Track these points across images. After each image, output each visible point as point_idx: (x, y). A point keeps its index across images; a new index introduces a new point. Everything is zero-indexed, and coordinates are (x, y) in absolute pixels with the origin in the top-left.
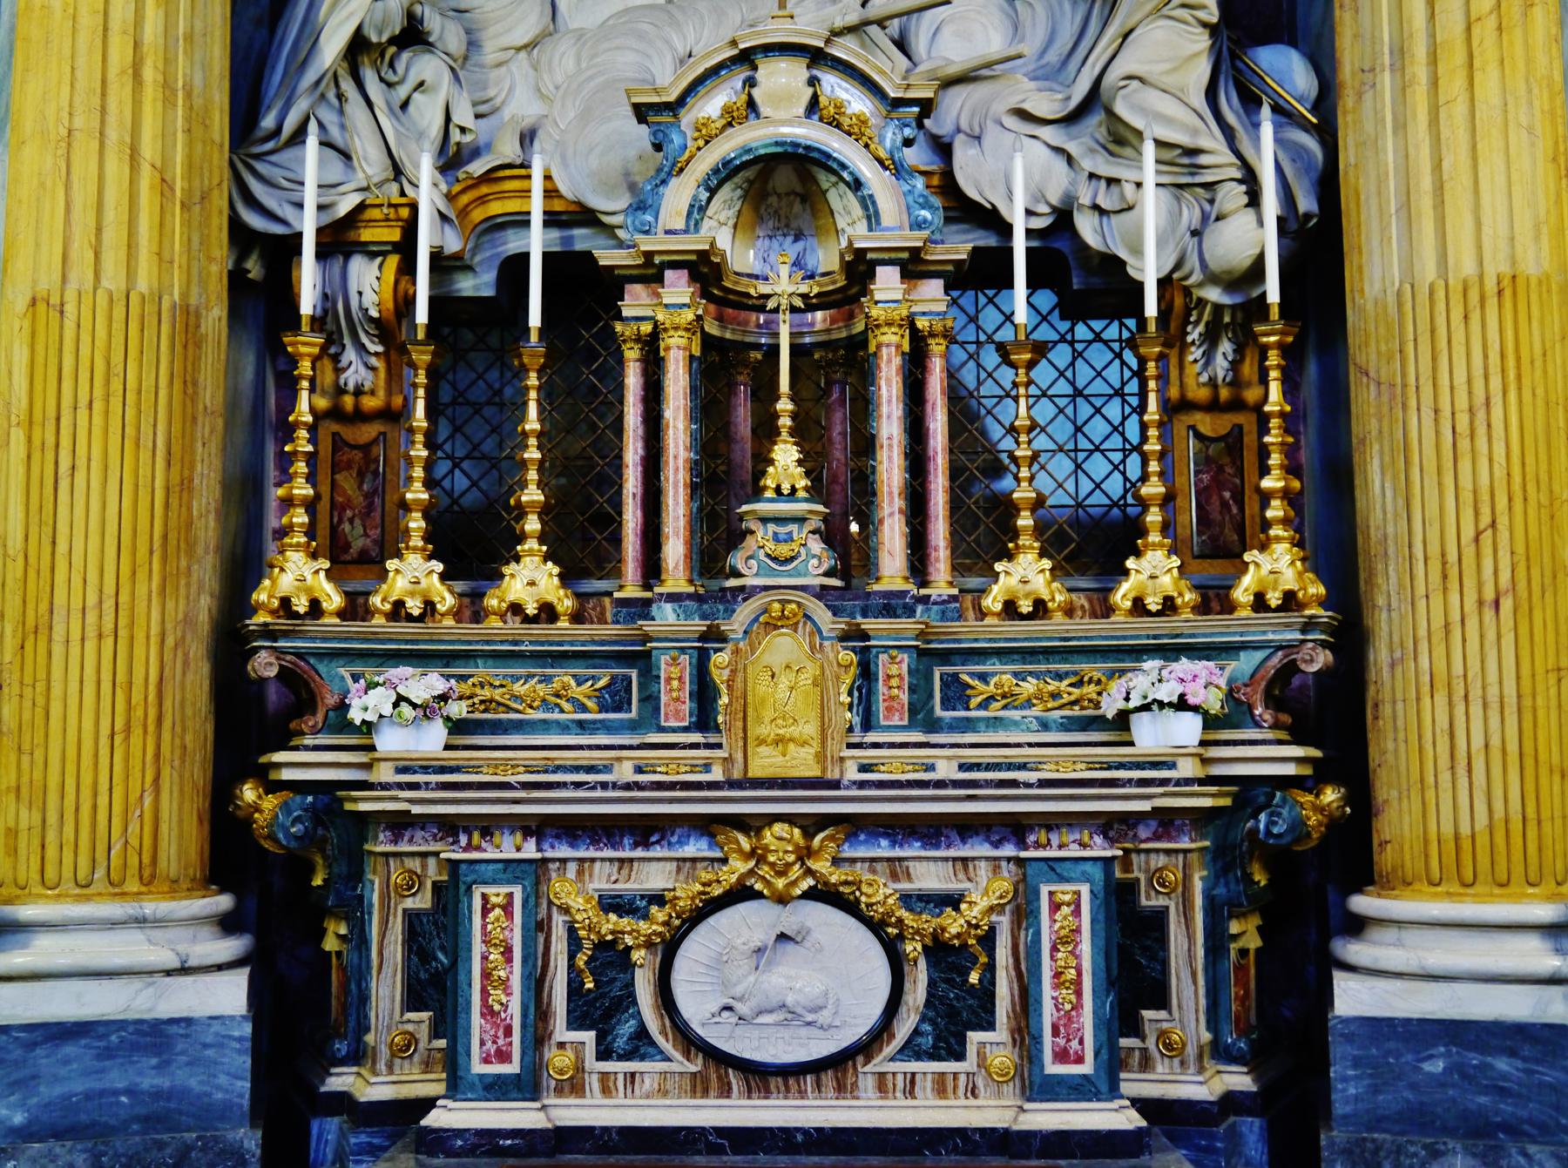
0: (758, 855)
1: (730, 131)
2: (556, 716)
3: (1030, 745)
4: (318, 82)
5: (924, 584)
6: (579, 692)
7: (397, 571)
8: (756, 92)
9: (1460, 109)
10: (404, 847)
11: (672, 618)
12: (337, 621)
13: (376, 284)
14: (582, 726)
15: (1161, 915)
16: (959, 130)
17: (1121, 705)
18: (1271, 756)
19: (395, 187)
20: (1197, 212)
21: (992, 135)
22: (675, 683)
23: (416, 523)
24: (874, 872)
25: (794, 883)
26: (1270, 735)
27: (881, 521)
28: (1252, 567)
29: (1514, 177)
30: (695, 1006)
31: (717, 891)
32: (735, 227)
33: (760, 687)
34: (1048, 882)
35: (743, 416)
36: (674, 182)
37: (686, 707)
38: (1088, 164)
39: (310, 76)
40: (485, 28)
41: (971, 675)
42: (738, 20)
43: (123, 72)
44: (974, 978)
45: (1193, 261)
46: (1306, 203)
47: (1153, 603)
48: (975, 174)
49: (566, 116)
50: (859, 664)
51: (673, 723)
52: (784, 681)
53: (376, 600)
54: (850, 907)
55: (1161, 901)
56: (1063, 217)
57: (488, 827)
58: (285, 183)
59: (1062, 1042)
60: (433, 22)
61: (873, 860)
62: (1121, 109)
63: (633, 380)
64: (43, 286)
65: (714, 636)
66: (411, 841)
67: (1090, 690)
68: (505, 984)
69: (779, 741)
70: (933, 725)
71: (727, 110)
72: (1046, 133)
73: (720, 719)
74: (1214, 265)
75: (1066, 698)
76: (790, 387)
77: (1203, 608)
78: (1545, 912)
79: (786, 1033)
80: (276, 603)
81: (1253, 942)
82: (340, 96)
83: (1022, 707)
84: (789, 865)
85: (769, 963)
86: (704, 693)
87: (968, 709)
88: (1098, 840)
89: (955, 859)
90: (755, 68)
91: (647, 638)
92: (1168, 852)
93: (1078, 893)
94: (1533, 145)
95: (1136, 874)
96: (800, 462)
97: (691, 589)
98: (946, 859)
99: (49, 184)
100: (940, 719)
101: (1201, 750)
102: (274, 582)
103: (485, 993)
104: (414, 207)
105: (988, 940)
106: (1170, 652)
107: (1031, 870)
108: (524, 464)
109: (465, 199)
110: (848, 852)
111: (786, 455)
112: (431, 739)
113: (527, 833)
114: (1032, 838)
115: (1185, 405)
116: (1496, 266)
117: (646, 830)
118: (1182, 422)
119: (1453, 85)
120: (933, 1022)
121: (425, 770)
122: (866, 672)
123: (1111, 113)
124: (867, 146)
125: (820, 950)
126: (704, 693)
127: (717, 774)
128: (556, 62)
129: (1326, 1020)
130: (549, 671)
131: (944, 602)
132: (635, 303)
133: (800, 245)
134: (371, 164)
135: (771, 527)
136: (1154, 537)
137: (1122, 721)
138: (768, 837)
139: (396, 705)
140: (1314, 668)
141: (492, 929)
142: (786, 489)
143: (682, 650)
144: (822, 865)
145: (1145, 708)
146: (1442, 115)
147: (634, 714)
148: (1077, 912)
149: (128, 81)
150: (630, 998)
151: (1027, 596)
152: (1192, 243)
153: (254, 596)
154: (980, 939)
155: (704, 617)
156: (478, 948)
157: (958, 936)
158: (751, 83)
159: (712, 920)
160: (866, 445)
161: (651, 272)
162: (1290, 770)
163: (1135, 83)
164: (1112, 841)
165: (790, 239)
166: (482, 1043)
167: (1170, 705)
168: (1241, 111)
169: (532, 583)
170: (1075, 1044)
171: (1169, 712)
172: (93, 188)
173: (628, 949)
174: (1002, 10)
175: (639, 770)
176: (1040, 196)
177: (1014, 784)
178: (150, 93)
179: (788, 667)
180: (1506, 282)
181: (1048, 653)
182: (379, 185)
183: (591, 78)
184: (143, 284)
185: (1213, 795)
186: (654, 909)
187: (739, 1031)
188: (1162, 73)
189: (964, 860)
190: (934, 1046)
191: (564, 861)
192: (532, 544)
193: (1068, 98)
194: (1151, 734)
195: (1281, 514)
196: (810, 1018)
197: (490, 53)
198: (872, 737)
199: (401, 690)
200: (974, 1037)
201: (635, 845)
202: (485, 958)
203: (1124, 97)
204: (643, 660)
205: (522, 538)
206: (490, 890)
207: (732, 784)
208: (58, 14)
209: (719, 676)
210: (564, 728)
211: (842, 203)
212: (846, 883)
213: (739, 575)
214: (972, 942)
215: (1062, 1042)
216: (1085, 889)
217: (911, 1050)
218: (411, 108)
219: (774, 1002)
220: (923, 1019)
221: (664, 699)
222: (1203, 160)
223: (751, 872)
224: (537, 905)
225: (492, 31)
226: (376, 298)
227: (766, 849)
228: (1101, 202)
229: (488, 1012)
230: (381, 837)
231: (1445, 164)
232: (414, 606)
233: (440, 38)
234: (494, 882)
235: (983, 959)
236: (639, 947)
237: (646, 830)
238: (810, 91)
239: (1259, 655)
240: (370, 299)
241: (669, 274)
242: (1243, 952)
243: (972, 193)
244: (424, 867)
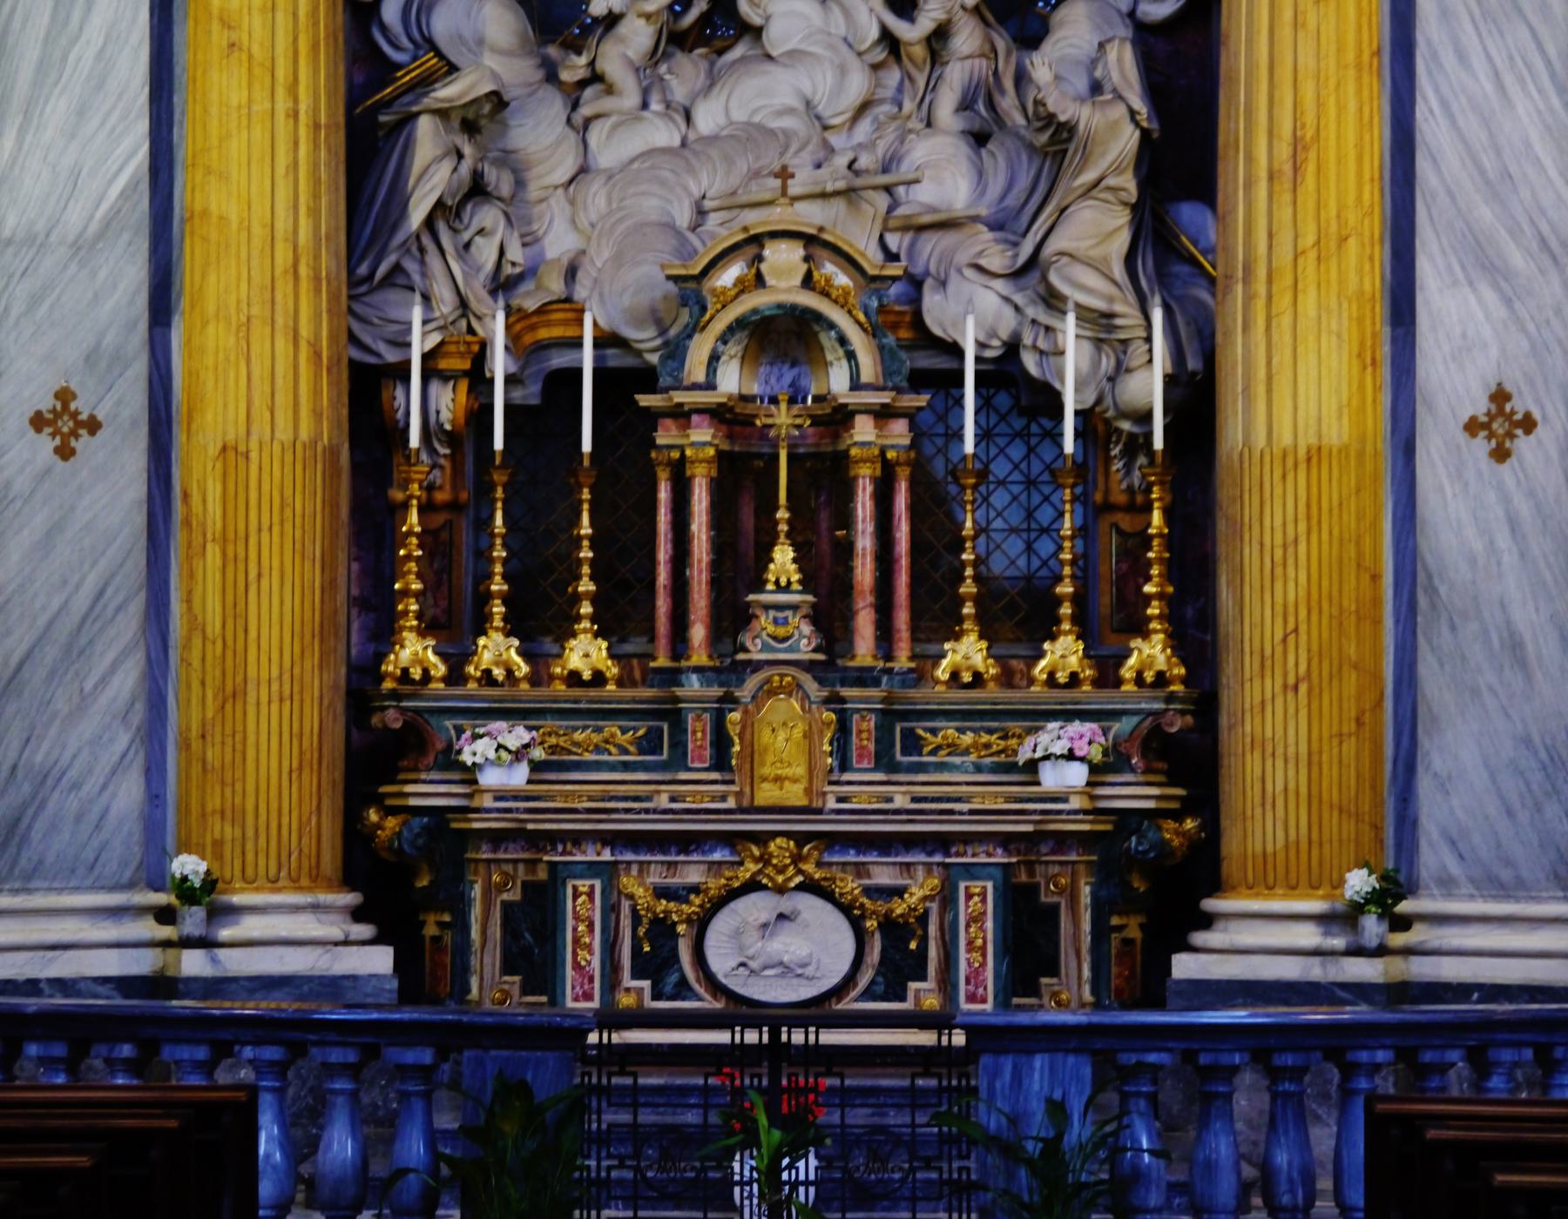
0: (765, 860)
1: (743, 297)
2: (605, 757)
3: (968, 784)
4: (405, 242)
5: (889, 657)
6: (622, 739)
7: (485, 647)
8: (764, 267)
9: (1286, 320)
10: (501, 856)
11: (696, 685)
12: (442, 685)
13: (451, 405)
14: (627, 767)
15: (1057, 906)
16: (927, 273)
17: (1029, 755)
18: (1134, 793)
19: (464, 323)
20: (1113, 361)
21: (954, 279)
22: (699, 735)
23: (498, 609)
24: (844, 871)
25: (790, 879)
26: (1141, 779)
27: (856, 613)
28: (1136, 653)
29: (1324, 373)
30: (721, 961)
31: (736, 884)
32: (743, 358)
33: (765, 736)
34: (966, 879)
35: (747, 517)
36: (697, 337)
37: (708, 753)
38: (1031, 312)
39: (400, 237)
40: (528, 169)
41: (925, 729)
42: (745, 169)
43: (286, 272)
44: (913, 945)
45: (1108, 401)
46: (1193, 363)
47: (1062, 677)
48: (938, 312)
49: (601, 256)
50: (839, 720)
51: (697, 765)
52: (782, 736)
53: (471, 669)
54: (827, 895)
55: (1055, 899)
56: (1013, 348)
57: (577, 839)
58: (376, 321)
59: (971, 988)
60: (491, 174)
61: (844, 864)
62: (1054, 279)
63: (664, 494)
64: (231, 437)
65: (729, 700)
66: (506, 851)
67: (1013, 742)
68: (589, 948)
69: (778, 779)
70: (894, 768)
71: (739, 281)
72: (999, 285)
73: (734, 762)
74: (1122, 406)
75: (995, 748)
76: (784, 484)
77: (1098, 683)
78: (1316, 906)
79: (784, 982)
80: (398, 672)
81: (1134, 932)
82: (422, 250)
83: (962, 754)
84: (786, 867)
85: (772, 934)
86: (721, 742)
87: (920, 754)
88: (999, 851)
89: (901, 864)
90: (762, 247)
91: (677, 700)
92: (1061, 863)
93: (985, 888)
94: (1340, 347)
95: (1038, 879)
96: (795, 560)
97: (711, 664)
98: (894, 864)
99: (232, 358)
100: (900, 763)
101: (1088, 789)
102: (397, 655)
103: (575, 954)
104: (483, 345)
105: (923, 919)
106: (1068, 716)
107: (953, 871)
108: (580, 562)
109: (518, 327)
110: (827, 858)
111: (783, 557)
112: (519, 776)
113: (605, 844)
114: (954, 850)
115: (1108, 507)
116: (1307, 439)
117: (687, 842)
118: (1104, 524)
119: (1283, 302)
120: (884, 975)
121: (516, 798)
122: (843, 728)
123: (1044, 278)
124: (850, 312)
125: (807, 926)
126: (721, 742)
127: (731, 803)
128: (589, 200)
129: (1164, 983)
130: (601, 723)
131: (904, 673)
132: (666, 436)
133: (795, 371)
134: (445, 303)
135: (772, 613)
136: (1066, 626)
137: (1032, 766)
138: (772, 847)
139: (497, 750)
140: (1174, 730)
141: (581, 904)
142: (783, 582)
143: (705, 710)
144: (809, 867)
145: (1046, 758)
146: (1274, 324)
147: (665, 756)
148: (984, 901)
149: (290, 278)
150: (675, 957)
151: (968, 669)
152: (1108, 387)
153: (383, 668)
154: (917, 918)
155: (721, 685)
156: (570, 923)
157: (902, 915)
158: (759, 258)
159: (732, 905)
160: (846, 550)
161: (682, 415)
162: (1151, 804)
163: (1065, 260)
164: (1008, 852)
165: (786, 366)
166: (573, 988)
167: (1062, 756)
168: (1154, 277)
169: (587, 655)
170: (981, 990)
171: (1062, 762)
172: (268, 363)
173: (675, 924)
174: (969, 158)
175: (673, 800)
176: (993, 334)
177: (951, 812)
178: (304, 285)
179: (784, 724)
180: (1314, 451)
181: (982, 715)
182: (453, 323)
183: (621, 220)
184: (304, 434)
185: (1091, 822)
186: (692, 897)
187: (750, 980)
188: (1093, 247)
189: (908, 865)
190: (885, 992)
191: (629, 863)
192: (586, 624)
193: (1016, 256)
194: (1055, 777)
195: (1157, 611)
196: (799, 971)
197: (533, 191)
198: (847, 777)
199: (500, 739)
200: (913, 986)
201: (678, 853)
202: (575, 929)
203: (1057, 270)
204: (675, 718)
205: (579, 618)
206: (579, 882)
207: (741, 810)
208: (234, 226)
209: (734, 731)
210: (612, 767)
211: (833, 353)
212: (825, 879)
213: (747, 651)
214: (912, 920)
215: (971, 988)
216: (990, 885)
217: (868, 994)
218: (473, 249)
219: (776, 960)
220: (877, 974)
221: (690, 746)
222: (1118, 322)
223: (760, 872)
224: (611, 893)
225: (535, 172)
226: (450, 416)
227: (771, 855)
228: (1041, 344)
229: (577, 966)
230: (484, 848)
231: (1275, 361)
232: (498, 673)
233: (497, 186)
234: (582, 877)
235: (920, 932)
236: (681, 922)
237: (687, 842)
238: (804, 267)
239: (1135, 720)
240: (446, 416)
241: (695, 418)
242: (1128, 942)
243: (937, 331)
244: (515, 870)
